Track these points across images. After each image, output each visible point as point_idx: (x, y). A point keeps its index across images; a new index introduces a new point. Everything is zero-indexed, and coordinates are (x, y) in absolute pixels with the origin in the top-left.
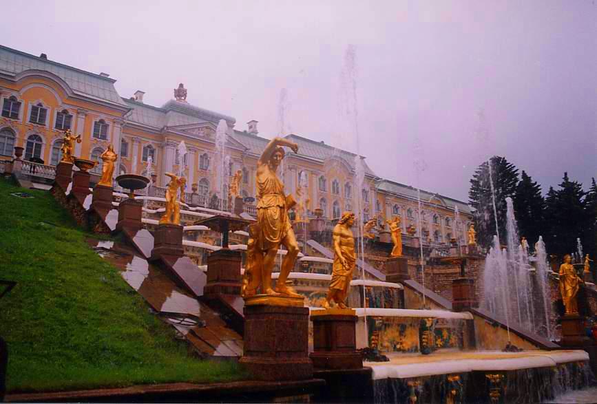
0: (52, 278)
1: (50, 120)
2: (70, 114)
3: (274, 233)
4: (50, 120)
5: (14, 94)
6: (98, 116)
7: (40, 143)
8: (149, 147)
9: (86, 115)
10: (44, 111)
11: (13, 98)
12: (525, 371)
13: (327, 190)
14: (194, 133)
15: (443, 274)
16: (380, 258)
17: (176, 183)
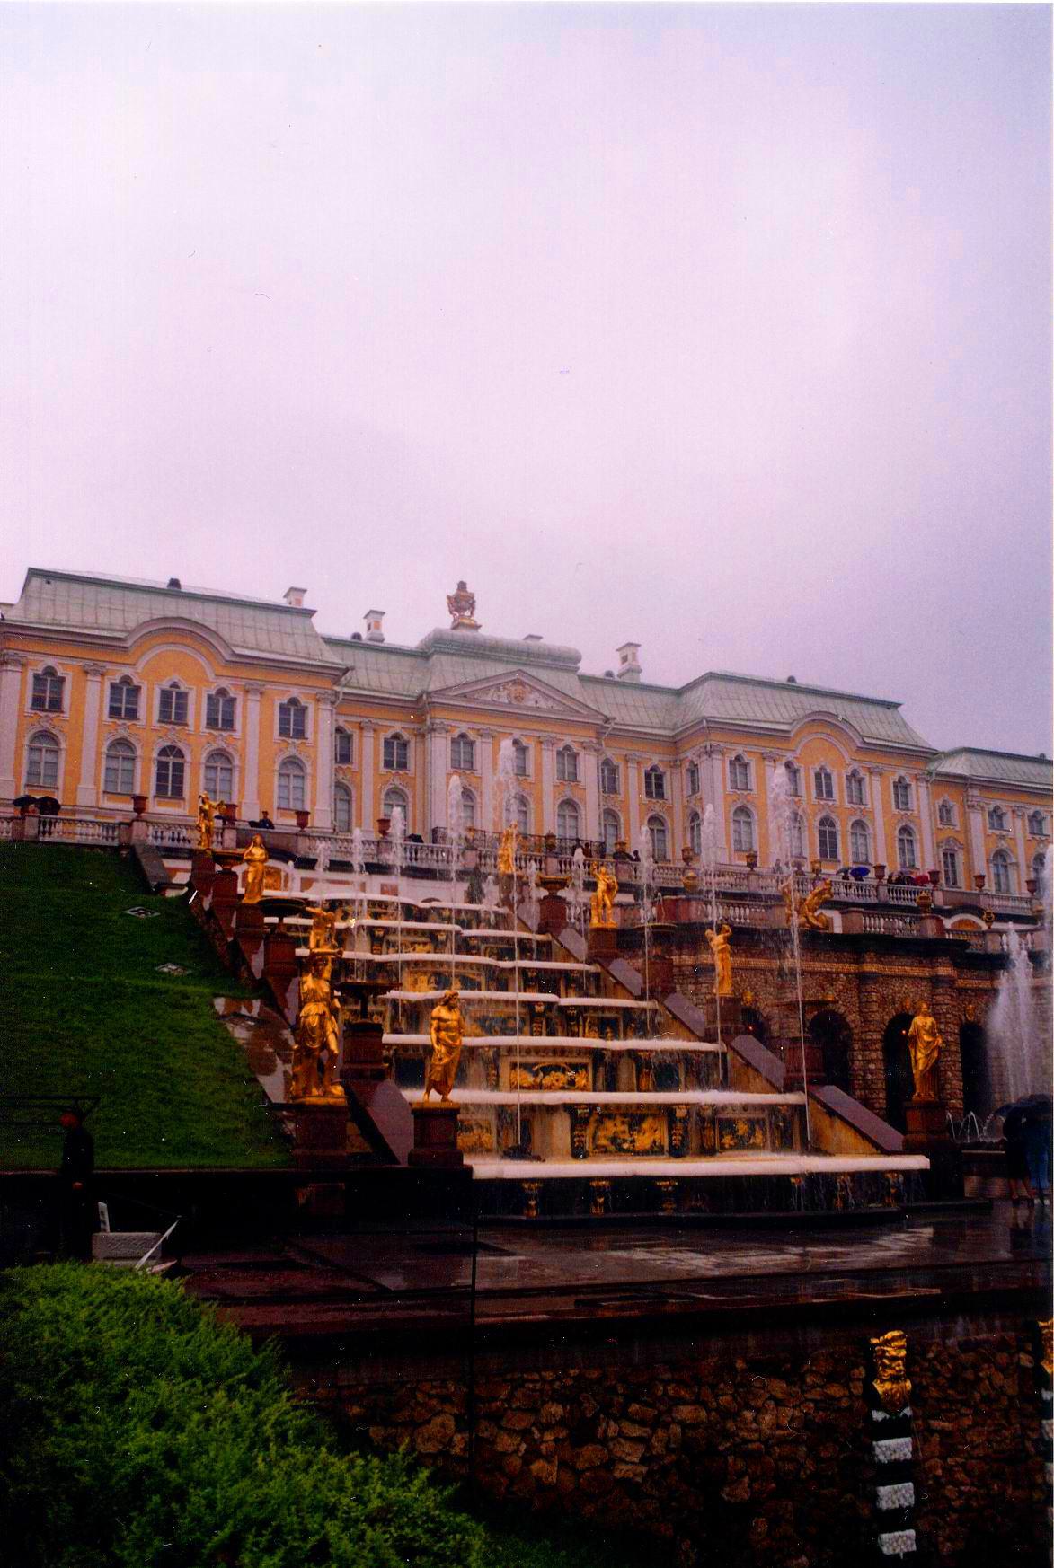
0: (158, 1067)
1: (197, 711)
2: (232, 695)
3: (313, 1040)
4: (197, 711)
5: (127, 671)
6: (284, 692)
7: (179, 760)
8: (396, 736)
9: (261, 693)
10: (182, 696)
11: (126, 680)
12: (748, 1177)
14: (489, 699)
16: (836, 967)
17: (322, 921)
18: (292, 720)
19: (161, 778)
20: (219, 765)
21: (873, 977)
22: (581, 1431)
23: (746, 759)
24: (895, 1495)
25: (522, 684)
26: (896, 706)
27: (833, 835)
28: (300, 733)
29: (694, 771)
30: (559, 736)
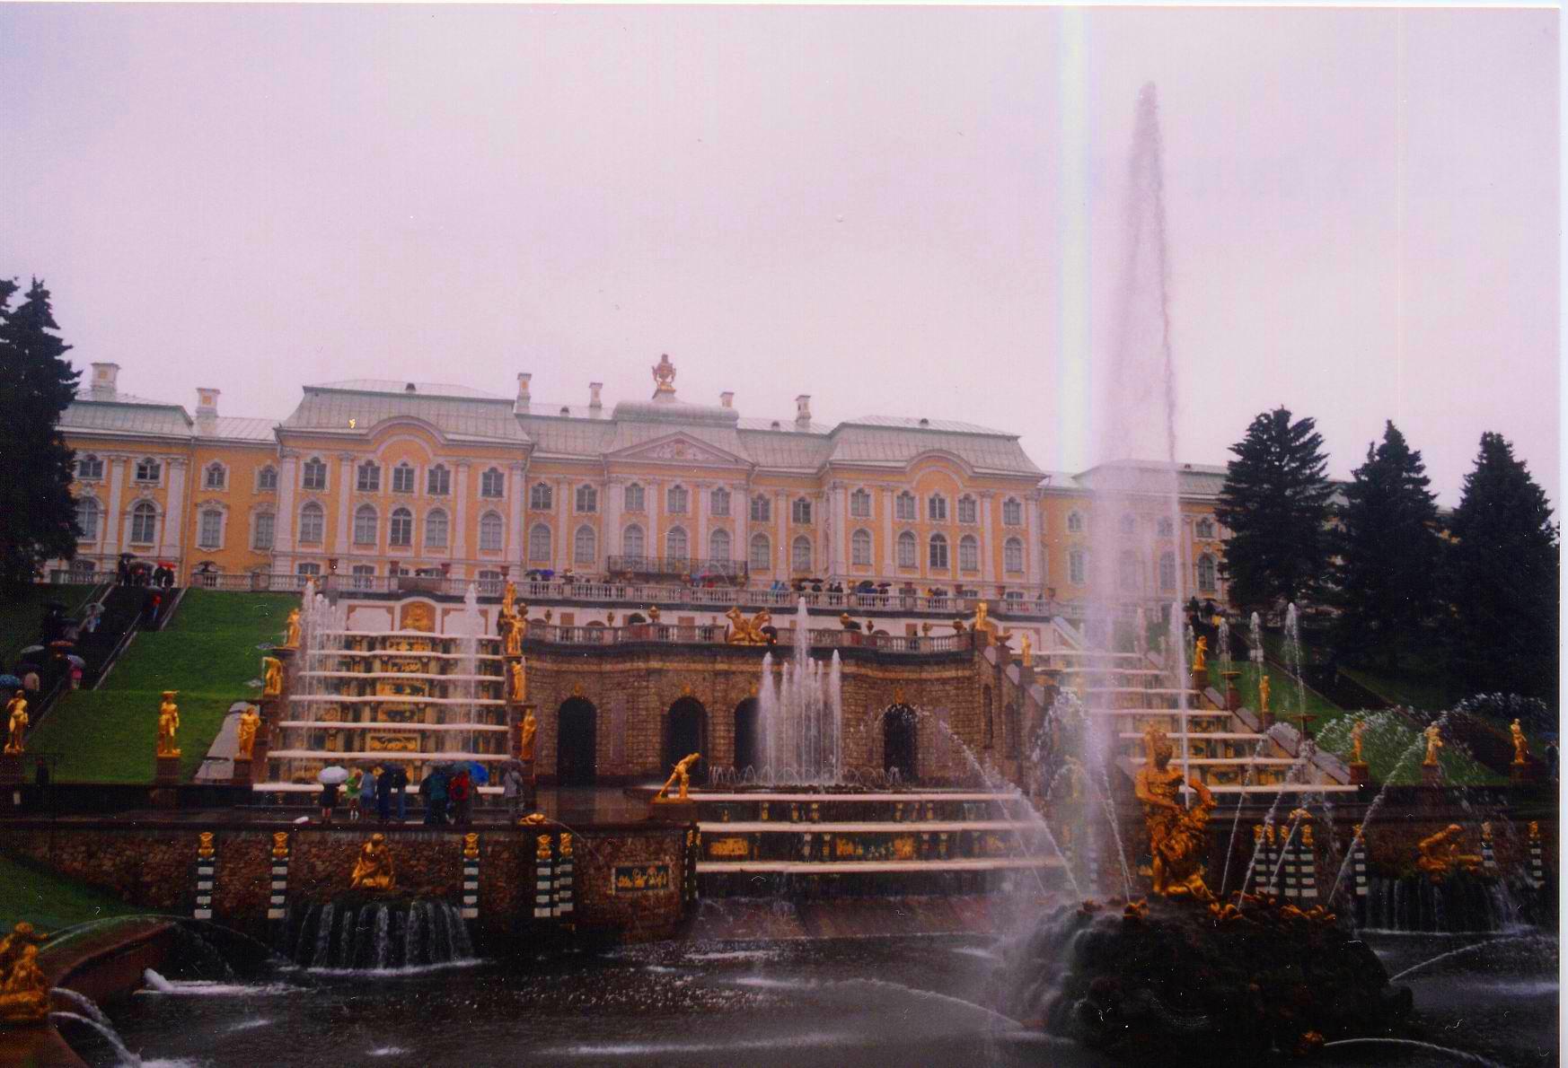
1: (421, 482)
4: (421, 482)
5: (370, 457)
7: (407, 518)
9: (469, 467)
10: (410, 472)
11: (370, 463)
13: (918, 516)
14: (655, 455)
15: (938, 680)
18: (493, 484)
19: (395, 531)
22: (91, 855)
23: (867, 491)
24: (202, 885)
25: (683, 442)
26: (1016, 438)
27: (943, 549)
28: (499, 493)
29: (828, 500)
30: (714, 481)
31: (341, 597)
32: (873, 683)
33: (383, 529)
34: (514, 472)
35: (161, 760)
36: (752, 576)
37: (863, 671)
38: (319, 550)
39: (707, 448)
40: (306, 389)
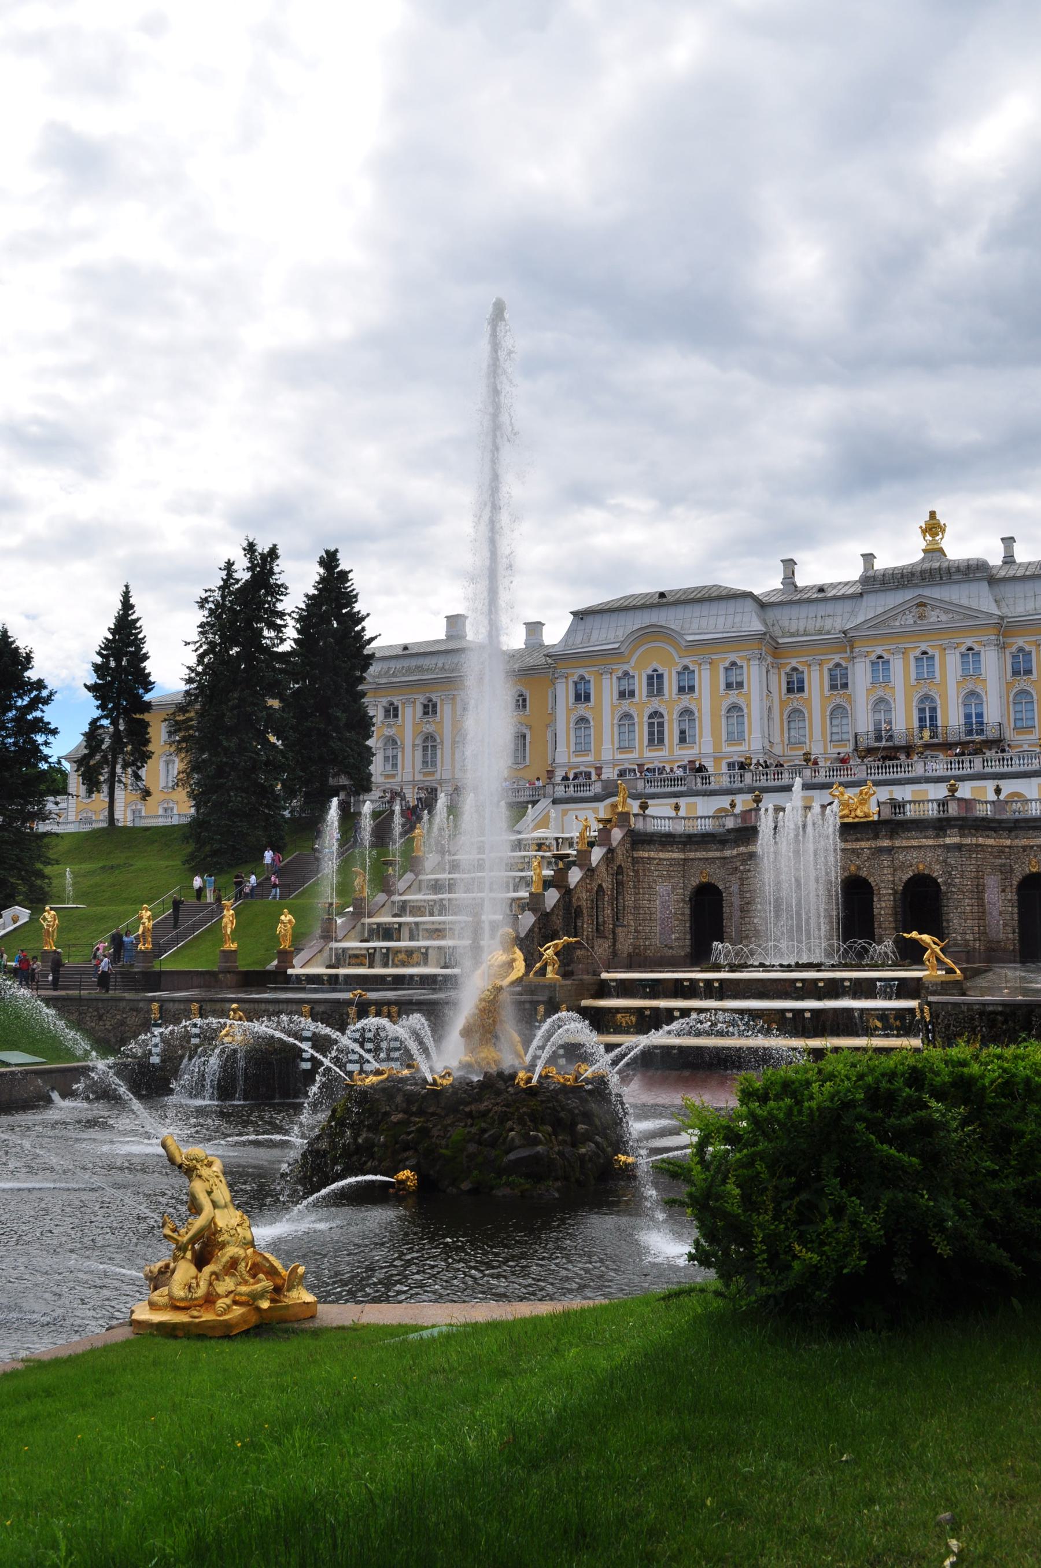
1: (670, 685)
5: (626, 667)
7: (660, 720)
10: (660, 677)
11: (626, 674)
14: (897, 623)
19: (651, 733)
20: (687, 718)
21: (889, 850)
25: (923, 605)
31: (555, 802)
32: (1001, 850)
33: (642, 732)
34: (752, 663)
35: (223, 951)
36: (1009, 735)
37: (968, 841)
38: (590, 758)
39: (948, 608)
40: (575, 614)
